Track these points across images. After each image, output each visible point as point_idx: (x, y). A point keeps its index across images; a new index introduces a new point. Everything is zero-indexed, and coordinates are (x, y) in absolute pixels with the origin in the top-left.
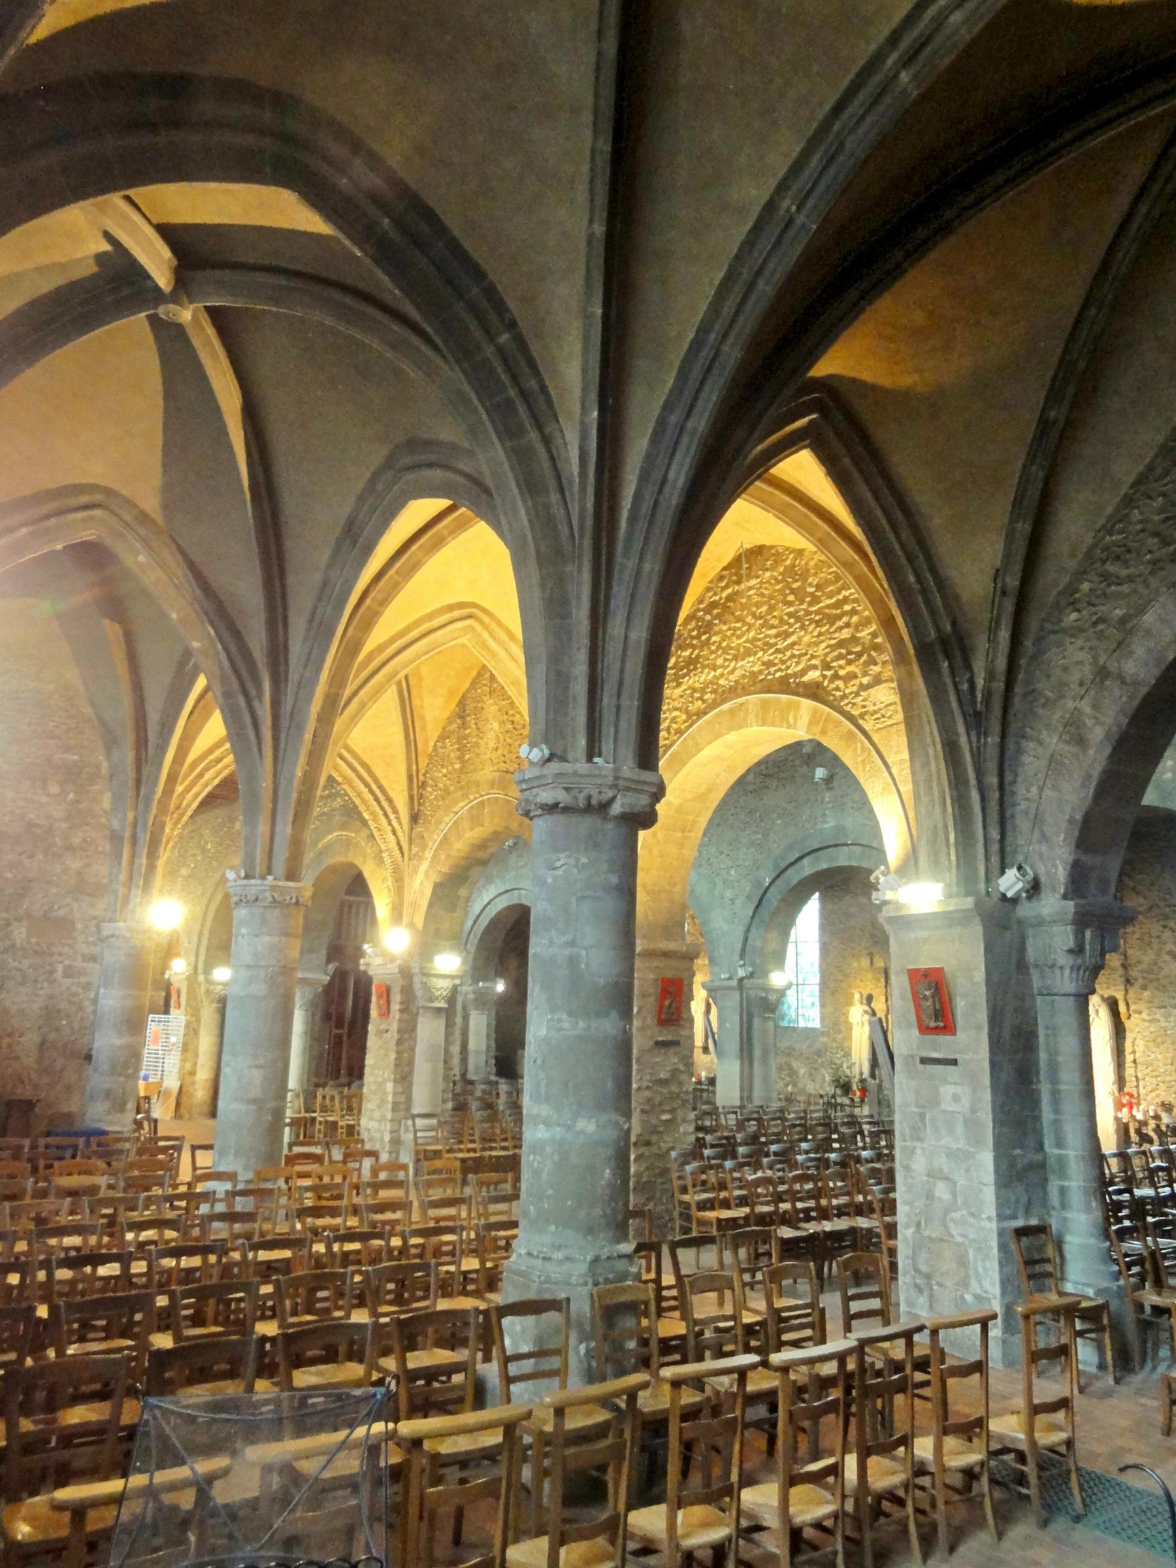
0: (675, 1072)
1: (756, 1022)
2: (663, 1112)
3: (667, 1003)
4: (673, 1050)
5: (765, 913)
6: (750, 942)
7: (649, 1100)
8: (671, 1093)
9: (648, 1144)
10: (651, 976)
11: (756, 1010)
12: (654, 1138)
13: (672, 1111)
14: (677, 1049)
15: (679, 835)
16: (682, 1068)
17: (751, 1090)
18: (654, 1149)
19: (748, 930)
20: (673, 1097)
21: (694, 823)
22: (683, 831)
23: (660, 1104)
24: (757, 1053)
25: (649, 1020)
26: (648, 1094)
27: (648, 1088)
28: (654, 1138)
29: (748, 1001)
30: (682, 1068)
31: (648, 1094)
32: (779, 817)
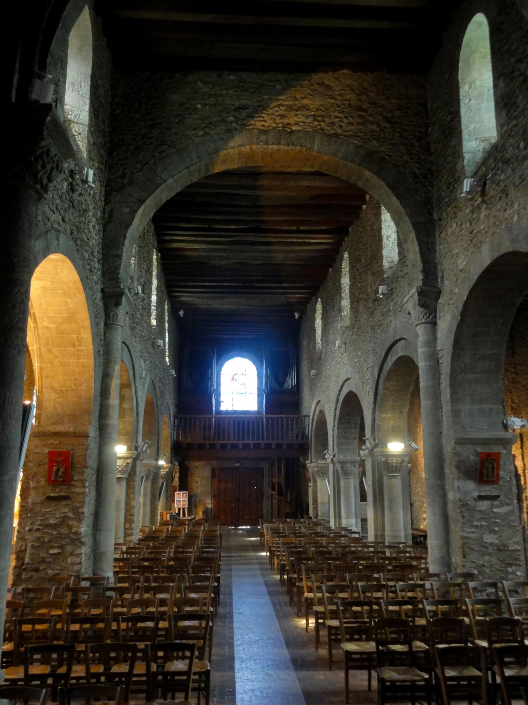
0: (65, 519)
1: (385, 478)
2: (53, 547)
3: (55, 468)
4: (64, 503)
5: (379, 398)
6: (376, 422)
7: (38, 539)
8: (59, 533)
9: (37, 570)
10: (47, 451)
11: (383, 471)
12: (42, 567)
13: (61, 547)
14: (69, 502)
15: (72, 349)
16: (71, 515)
17: (384, 530)
18: (42, 574)
19: (374, 412)
20: (61, 537)
21: (79, 339)
22: (74, 345)
23: (49, 541)
24: (386, 503)
25: (43, 482)
26: (38, 534)
27: (38, 530)
28: (42, 567)
29: (378, 464)
30: (71, 515)
31: (38, 534)
32: (379, 329)
